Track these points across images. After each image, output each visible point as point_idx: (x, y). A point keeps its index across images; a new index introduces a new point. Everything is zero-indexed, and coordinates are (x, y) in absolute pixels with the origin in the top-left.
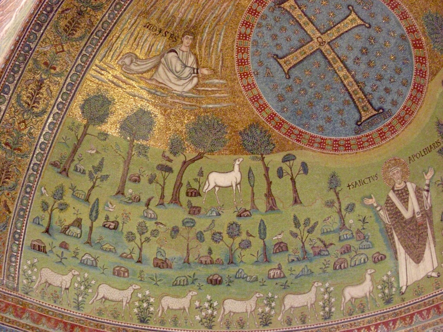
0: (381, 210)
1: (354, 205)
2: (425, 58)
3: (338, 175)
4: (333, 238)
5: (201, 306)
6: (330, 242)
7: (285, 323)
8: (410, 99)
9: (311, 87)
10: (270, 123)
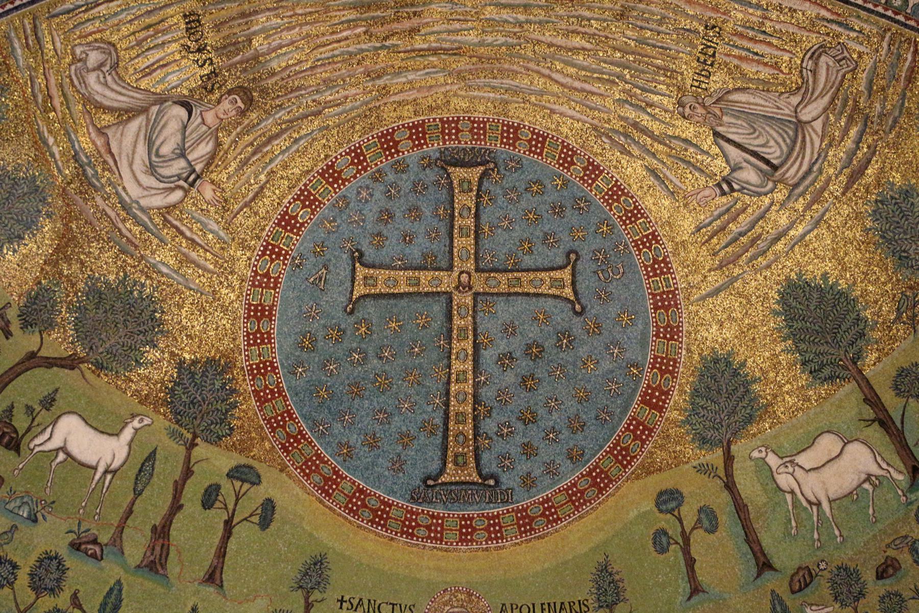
3: (330, 566)
8: (567, 490)
9: (381, 358)
10: (253, 380)
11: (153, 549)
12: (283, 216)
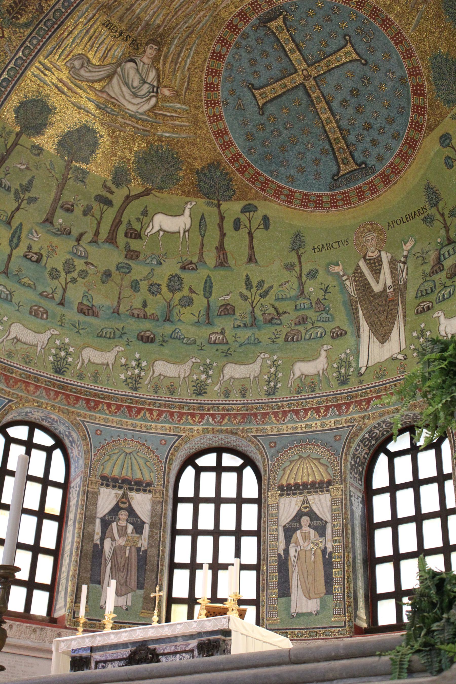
0: (348, 280)
1: (317, 271)
2: (424, 108)
4: (288, 306)
5: (127, 365)
6: (285, 310)
7: (222, 395)
8: (398, 155)
9: (287, 129)
11: (219, 257)
12: (206, 85)
